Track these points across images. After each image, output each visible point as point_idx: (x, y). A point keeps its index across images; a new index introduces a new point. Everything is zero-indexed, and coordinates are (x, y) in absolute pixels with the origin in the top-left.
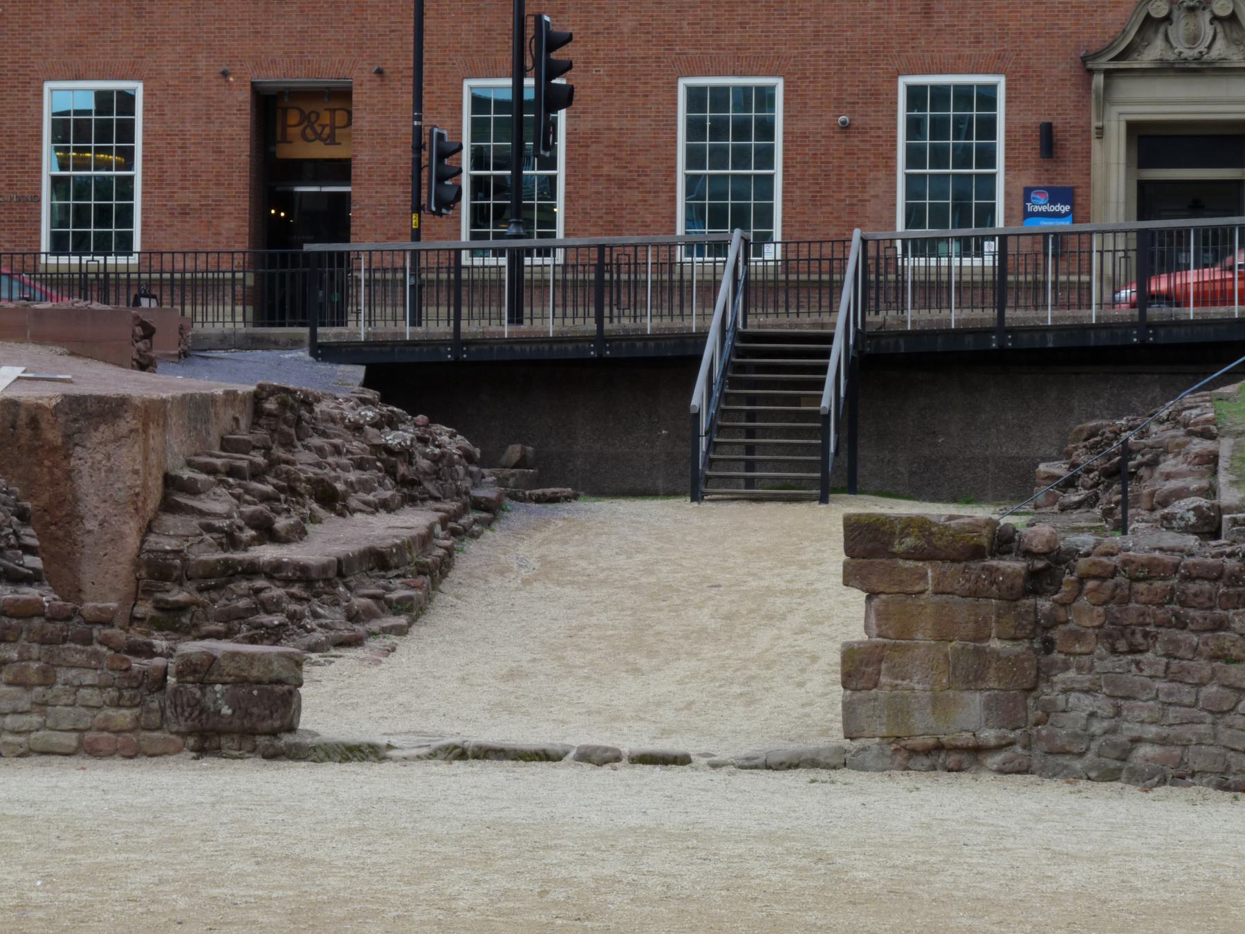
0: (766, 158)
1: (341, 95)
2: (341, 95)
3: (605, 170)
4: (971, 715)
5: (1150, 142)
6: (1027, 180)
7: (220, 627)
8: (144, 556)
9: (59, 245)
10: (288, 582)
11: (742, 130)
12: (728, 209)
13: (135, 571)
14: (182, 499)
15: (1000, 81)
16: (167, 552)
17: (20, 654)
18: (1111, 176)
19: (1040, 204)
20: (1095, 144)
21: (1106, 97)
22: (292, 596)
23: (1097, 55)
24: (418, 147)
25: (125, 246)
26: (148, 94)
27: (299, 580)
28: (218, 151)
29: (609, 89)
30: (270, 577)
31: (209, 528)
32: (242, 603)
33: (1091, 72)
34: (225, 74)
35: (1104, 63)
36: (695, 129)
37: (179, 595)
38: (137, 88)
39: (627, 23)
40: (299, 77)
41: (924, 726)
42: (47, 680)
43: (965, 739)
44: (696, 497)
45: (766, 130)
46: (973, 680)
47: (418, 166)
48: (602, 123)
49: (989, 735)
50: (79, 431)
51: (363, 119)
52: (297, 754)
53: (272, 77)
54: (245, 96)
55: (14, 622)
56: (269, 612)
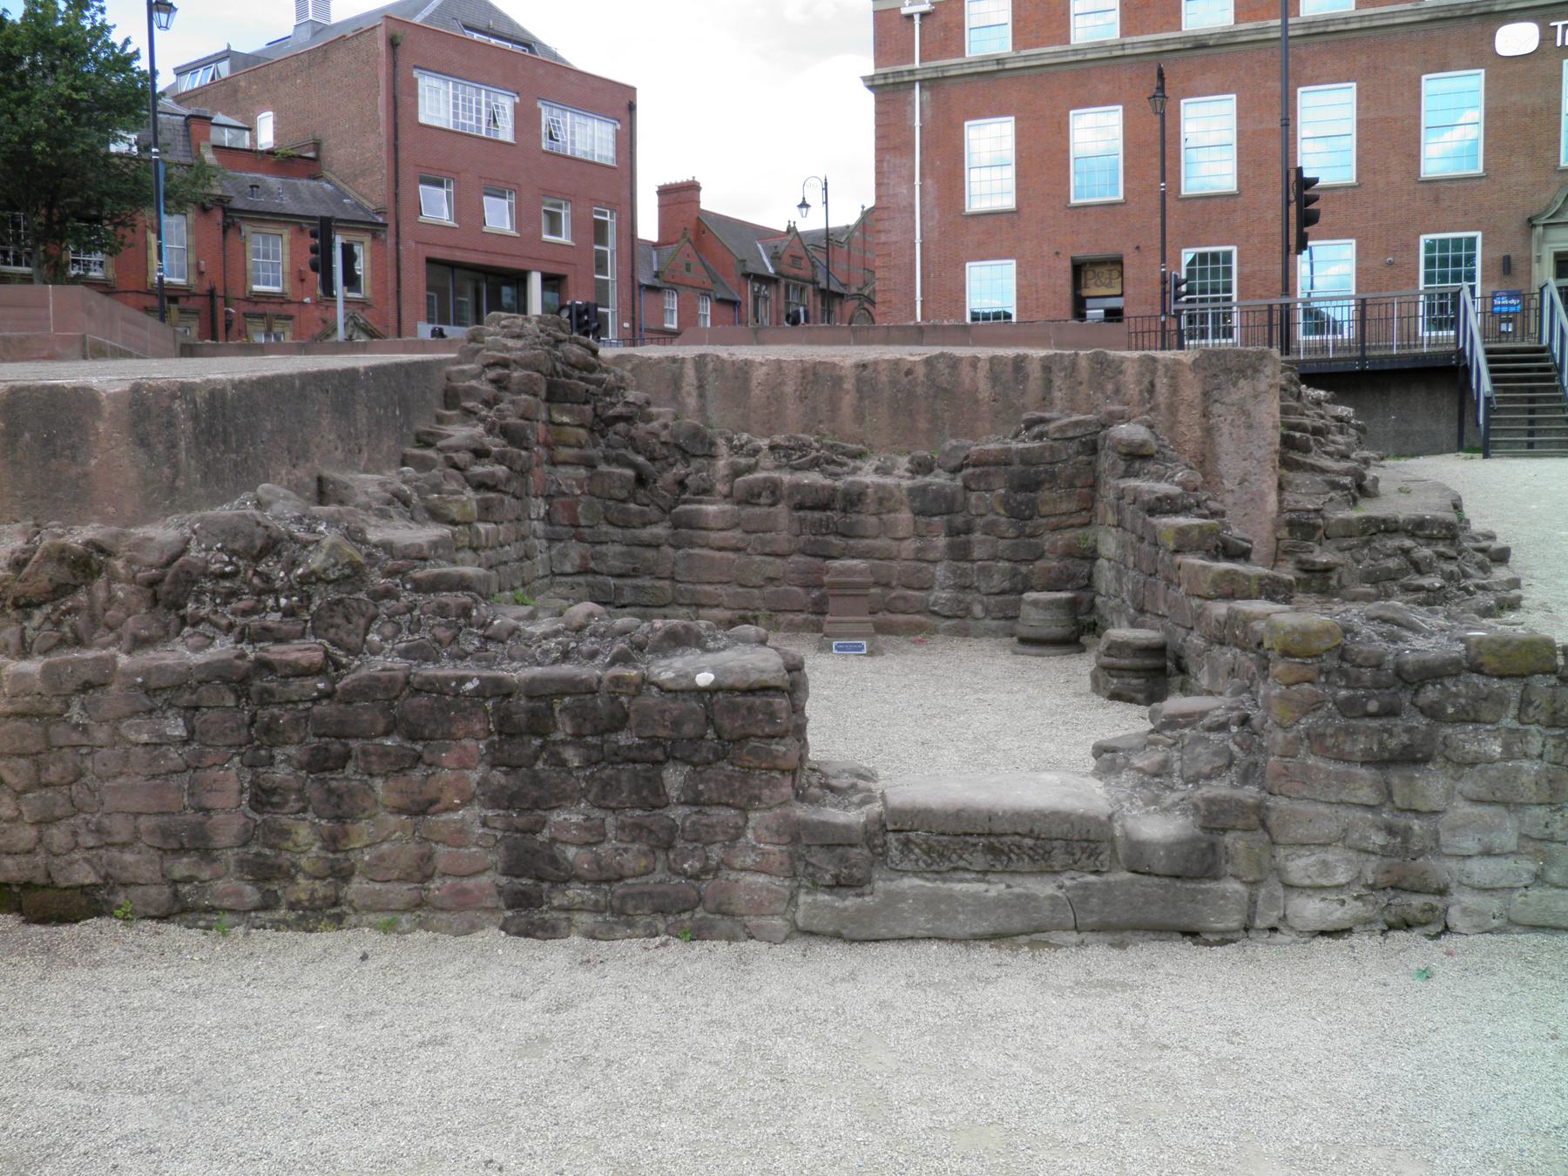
1: (1117, 262)
2: (1117, 262)
6: (1493, 287)
7: (1367, 588)
8: (1287, 516)
10: (1431, 539)
13: (1274, 532)
14: (1297, 456)
15: (1479, 235)
16: (1309, 511)
17: (1507, 747)
20: (1535, 266)
21: (1542, 240)
22: (1441, 555)
23: (1538, 216)
24: (1164, 282)
27: (1444, 538)
30: (1412, 535)
31: (1335, 486)
32: (1392, 563)
33: (1534, 226)
35: (1543, 220)
37: (1322, 556)
44: (1486, 456)
47: (1164, 292)
50: (1219, 388)
51: (1128, 272)
53: (1082, 253)
54: (1068, 264)
55: (1496, 684)
56: (1420, 572)
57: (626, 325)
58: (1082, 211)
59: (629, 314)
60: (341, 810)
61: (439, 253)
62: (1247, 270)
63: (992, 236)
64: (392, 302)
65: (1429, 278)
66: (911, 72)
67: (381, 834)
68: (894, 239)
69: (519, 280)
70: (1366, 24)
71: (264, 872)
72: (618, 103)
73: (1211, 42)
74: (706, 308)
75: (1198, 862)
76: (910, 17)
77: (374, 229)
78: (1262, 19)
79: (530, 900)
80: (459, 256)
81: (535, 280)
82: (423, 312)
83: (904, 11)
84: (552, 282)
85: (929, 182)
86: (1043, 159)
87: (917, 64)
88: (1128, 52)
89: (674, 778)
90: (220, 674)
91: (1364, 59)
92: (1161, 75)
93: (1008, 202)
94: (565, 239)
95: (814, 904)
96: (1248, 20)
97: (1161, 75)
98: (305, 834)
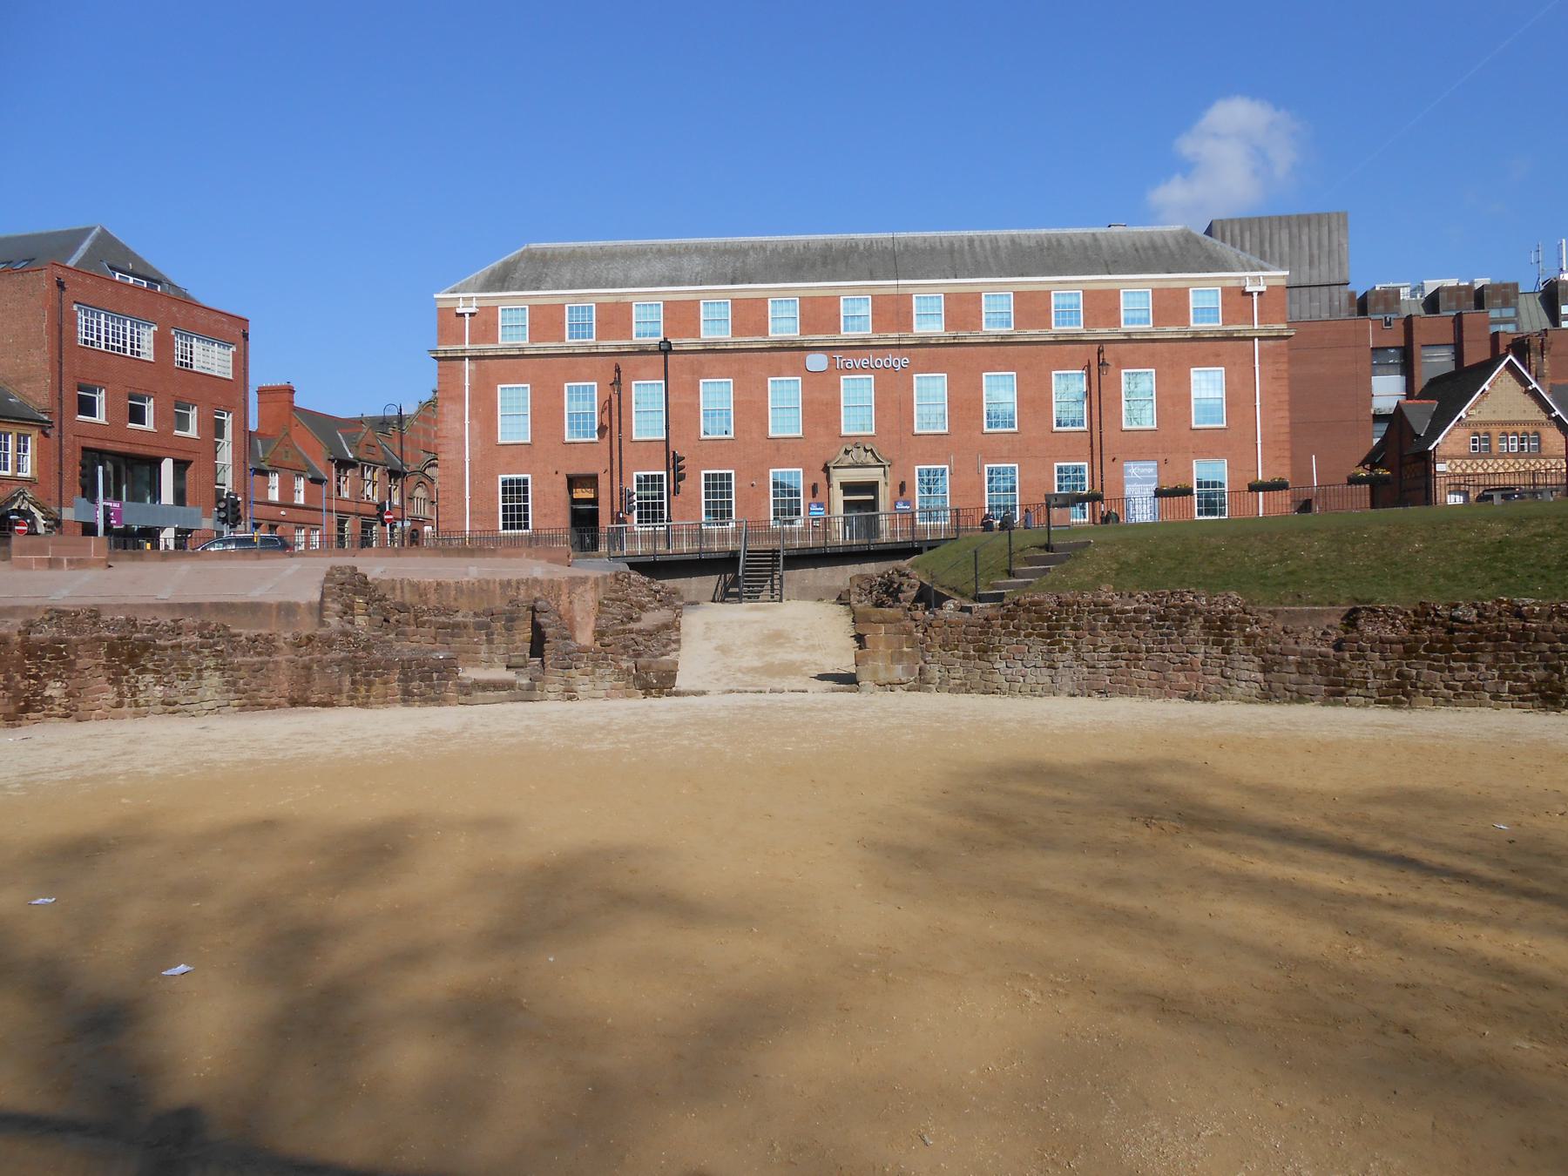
0: (729, 495)
4: (898, 672)
5: (848, 488)
9: (505, 527)
11: (722, 486)
12: (720, 512)
18: (838, 498)
19: (814, 508)
25: (526, 527)
36: (707, 487)
37: (607, 640)
38: (703, 473)
40: (581, 472)
41: (883, 677)
42: (593, 673)
43: (896, 680)
45: (729, 485)
46: (899, 661)
49: (904, 679)
52: (677, 694)
53: (572, 472)
60: (370, 684)
61: (92, 444)
64: (55, 482)
65: (775, 494)
67: (378, 688)
69: (156, 463)
71: (351, 698)
72: (232, 331)
74: (300, 484)
75: (532, 688)
76: (463, 315)
77: (44, 427)
79: (407, 698)
80: (109, 446)
81: (167, 467)
82: (79, 489)
83: (459, 311)
84: (181, 467)
87: (467, 346)
89: (435, 675)
90: (343, 659)
92: (618, 370)
94: (192, 432)
95: (462, 698)
97: (618, 370)
98: (363, 689)
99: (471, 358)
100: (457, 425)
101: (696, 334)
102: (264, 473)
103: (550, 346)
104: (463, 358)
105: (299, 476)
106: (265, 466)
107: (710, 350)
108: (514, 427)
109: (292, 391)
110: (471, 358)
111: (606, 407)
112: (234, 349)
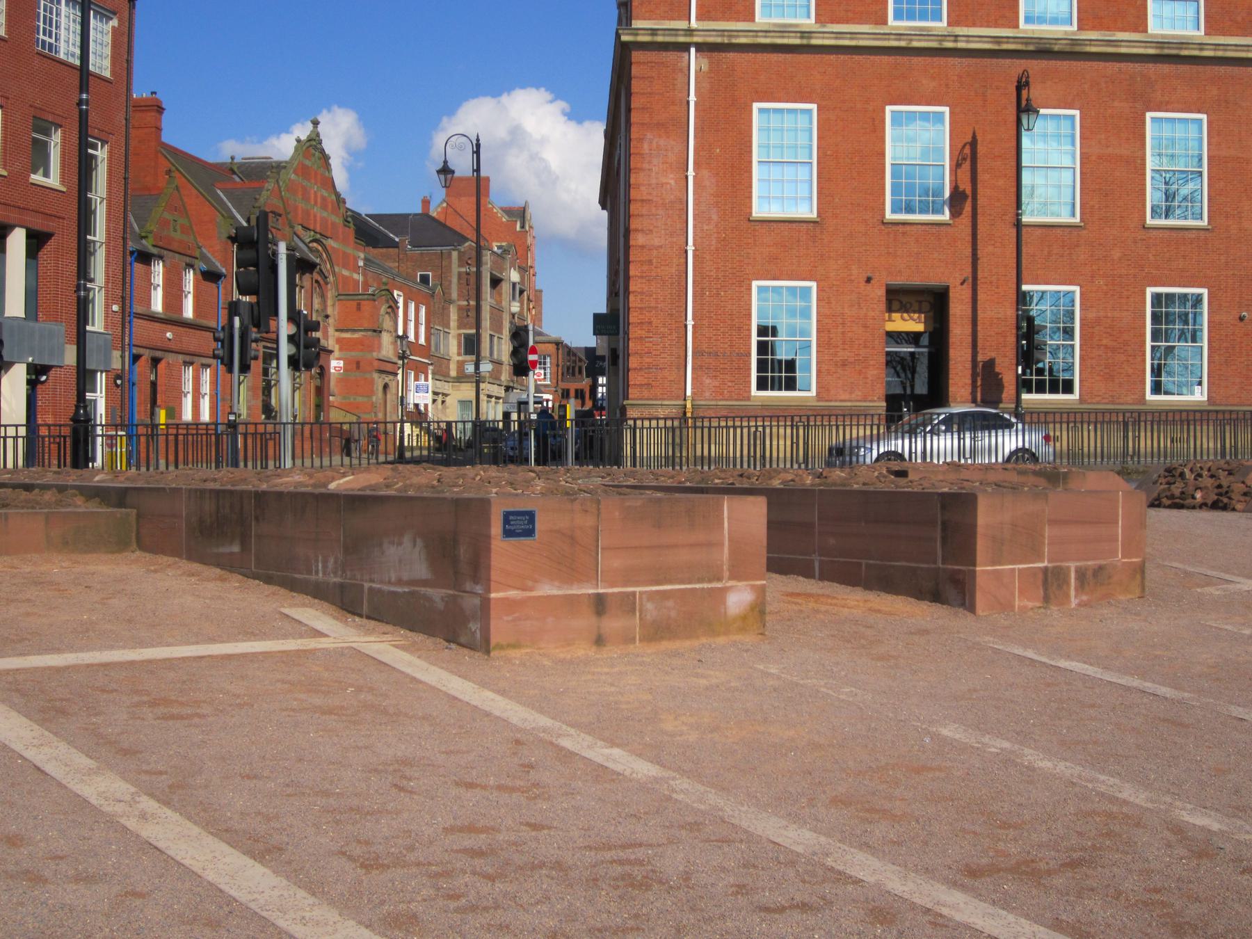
3: (1104, 342)
11: (1169, 318)
26: (819, 290)
28: (865, 326)
29: (1106, 293)
34: (869, 280)
39: (1116, 254)
48: (1102, 314)
54: (881, 293)
57: (115, 308)
58: (901, 229)
59: (119, 293)
62: (1092, 315)
63: (787, 246)
66: (690, 32)
68: (656, 242)
70: (1220, 54)
73: (1056, 48)
78: (1108, 29)
85: (705, 173)
86: (849, 160)
87: (694, 24)
88: (961, 45)
91: (1215, 92)
93: (806, 210)
94: (54, 181)
96: (1093, 28)
99: (700, 47)
100: (671, 180)
101: (1140, 24)
102: (145, 258)
103: (861, 32)
104: (685, 47)
105: (190, 266)
106: (148, 245)
107: (1171, 56)
108: (784, 186)
109: (160, 109)
110: (700, 47)
111: (968, 155)
112: (114, 22)
